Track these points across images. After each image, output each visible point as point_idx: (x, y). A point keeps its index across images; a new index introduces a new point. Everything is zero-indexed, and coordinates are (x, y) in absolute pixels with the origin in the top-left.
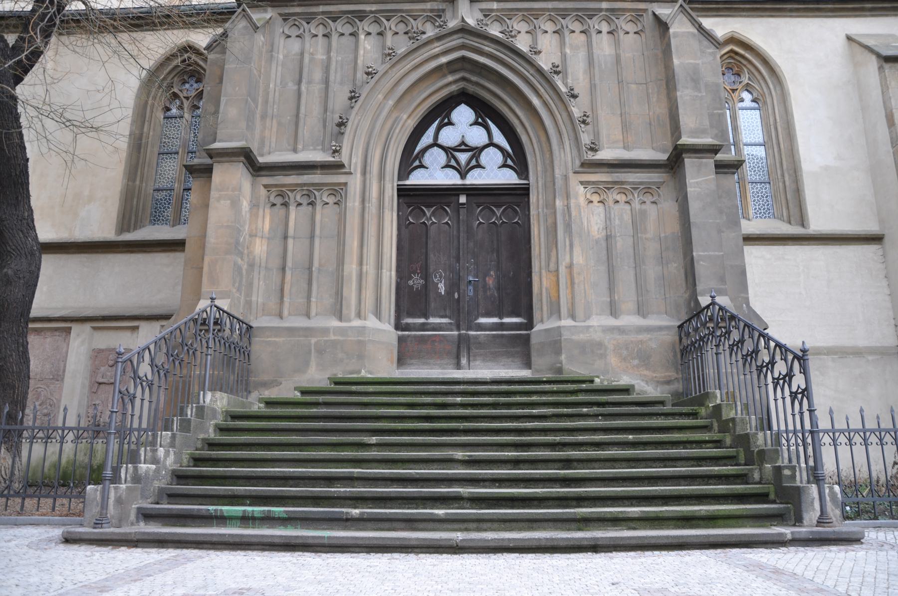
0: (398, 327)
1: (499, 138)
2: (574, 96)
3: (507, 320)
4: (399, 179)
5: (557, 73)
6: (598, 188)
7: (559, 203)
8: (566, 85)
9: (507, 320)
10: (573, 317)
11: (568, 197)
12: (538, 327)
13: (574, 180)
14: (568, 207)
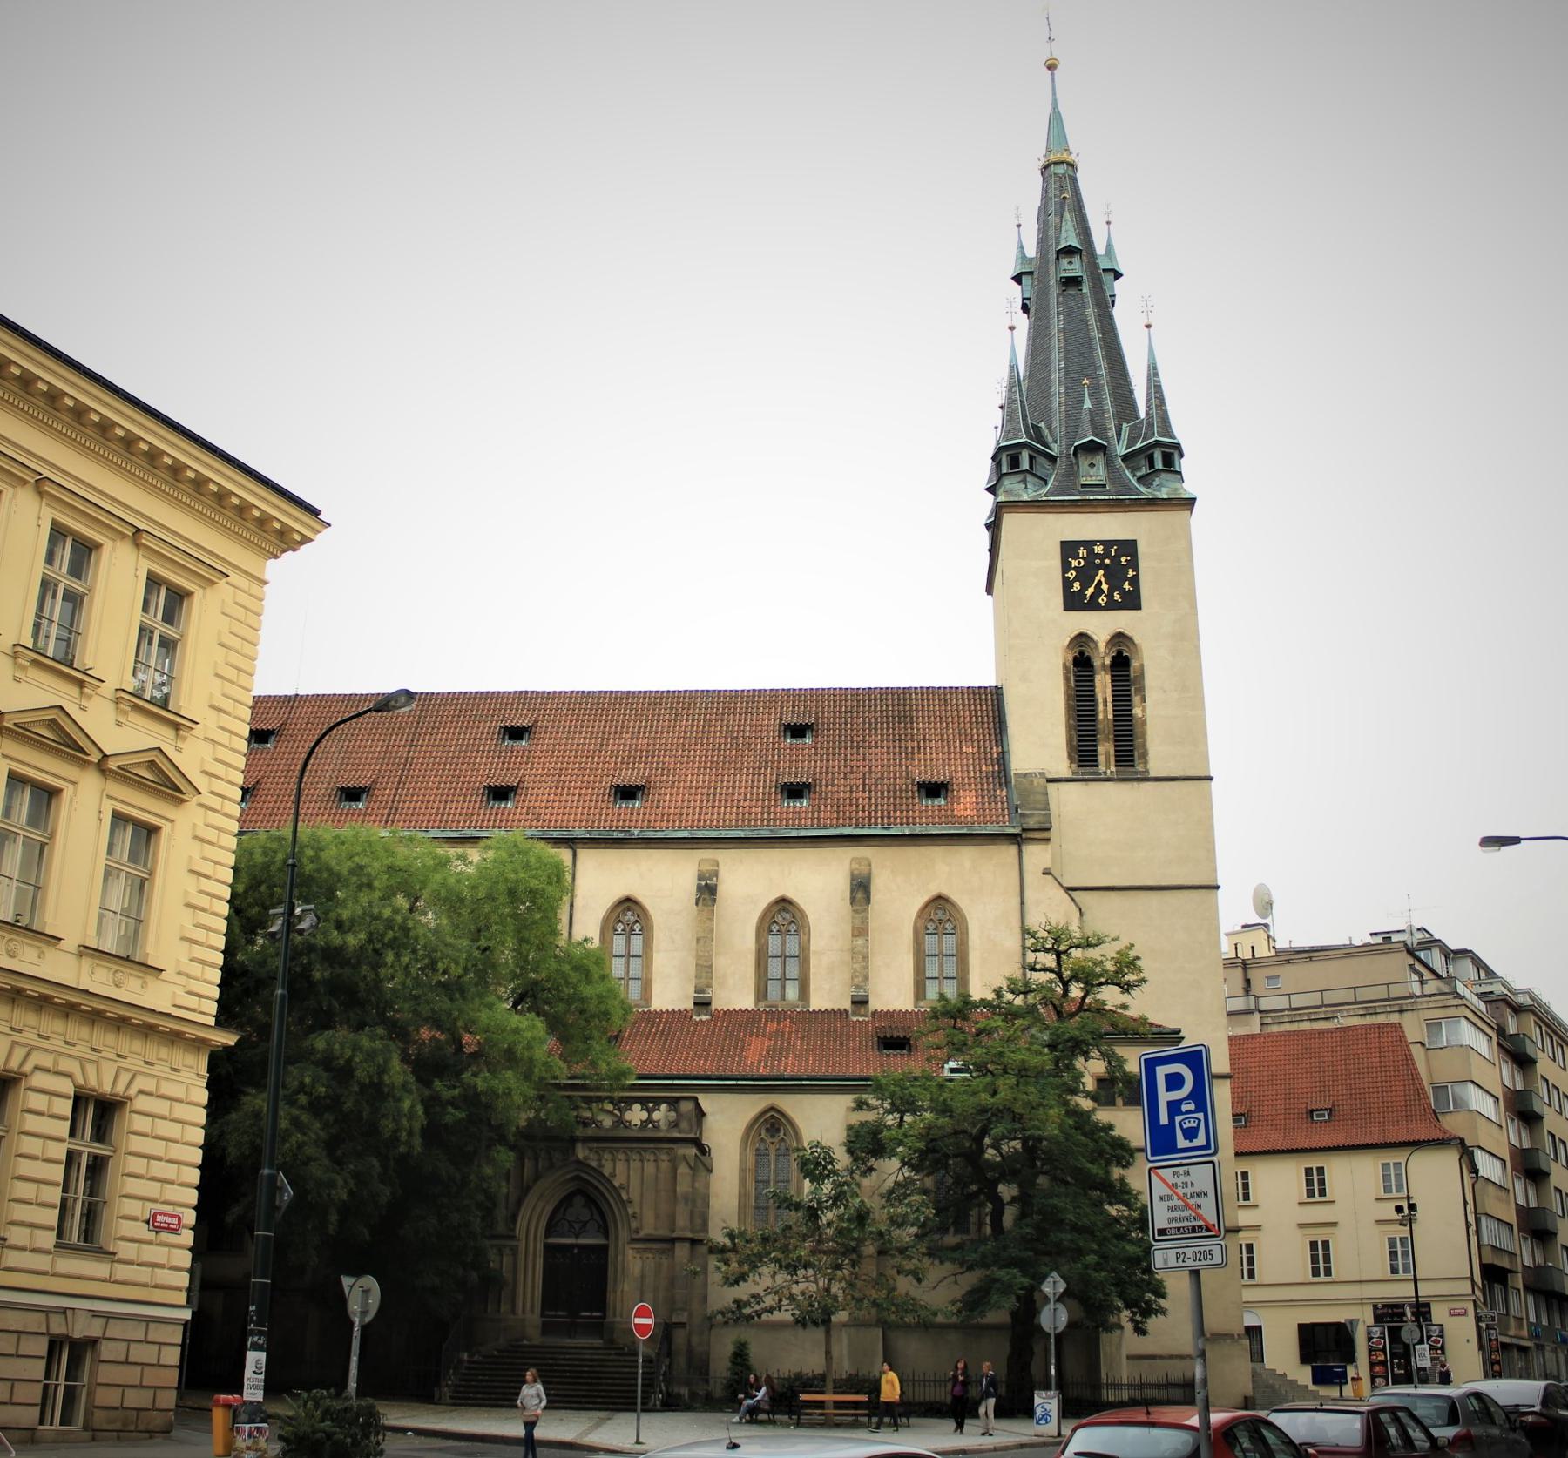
0: (542, 1315)
1: (597, 1217)
3: (595, 1314)
4: (547, 1235)
6: (638, 1251)
7: (620, 1258)
8: (628, 1193)
9: (595, 1314)
11: (624, 1255)
12: (607, 1320)
13: (627, 1247)
14: (623, 1261)
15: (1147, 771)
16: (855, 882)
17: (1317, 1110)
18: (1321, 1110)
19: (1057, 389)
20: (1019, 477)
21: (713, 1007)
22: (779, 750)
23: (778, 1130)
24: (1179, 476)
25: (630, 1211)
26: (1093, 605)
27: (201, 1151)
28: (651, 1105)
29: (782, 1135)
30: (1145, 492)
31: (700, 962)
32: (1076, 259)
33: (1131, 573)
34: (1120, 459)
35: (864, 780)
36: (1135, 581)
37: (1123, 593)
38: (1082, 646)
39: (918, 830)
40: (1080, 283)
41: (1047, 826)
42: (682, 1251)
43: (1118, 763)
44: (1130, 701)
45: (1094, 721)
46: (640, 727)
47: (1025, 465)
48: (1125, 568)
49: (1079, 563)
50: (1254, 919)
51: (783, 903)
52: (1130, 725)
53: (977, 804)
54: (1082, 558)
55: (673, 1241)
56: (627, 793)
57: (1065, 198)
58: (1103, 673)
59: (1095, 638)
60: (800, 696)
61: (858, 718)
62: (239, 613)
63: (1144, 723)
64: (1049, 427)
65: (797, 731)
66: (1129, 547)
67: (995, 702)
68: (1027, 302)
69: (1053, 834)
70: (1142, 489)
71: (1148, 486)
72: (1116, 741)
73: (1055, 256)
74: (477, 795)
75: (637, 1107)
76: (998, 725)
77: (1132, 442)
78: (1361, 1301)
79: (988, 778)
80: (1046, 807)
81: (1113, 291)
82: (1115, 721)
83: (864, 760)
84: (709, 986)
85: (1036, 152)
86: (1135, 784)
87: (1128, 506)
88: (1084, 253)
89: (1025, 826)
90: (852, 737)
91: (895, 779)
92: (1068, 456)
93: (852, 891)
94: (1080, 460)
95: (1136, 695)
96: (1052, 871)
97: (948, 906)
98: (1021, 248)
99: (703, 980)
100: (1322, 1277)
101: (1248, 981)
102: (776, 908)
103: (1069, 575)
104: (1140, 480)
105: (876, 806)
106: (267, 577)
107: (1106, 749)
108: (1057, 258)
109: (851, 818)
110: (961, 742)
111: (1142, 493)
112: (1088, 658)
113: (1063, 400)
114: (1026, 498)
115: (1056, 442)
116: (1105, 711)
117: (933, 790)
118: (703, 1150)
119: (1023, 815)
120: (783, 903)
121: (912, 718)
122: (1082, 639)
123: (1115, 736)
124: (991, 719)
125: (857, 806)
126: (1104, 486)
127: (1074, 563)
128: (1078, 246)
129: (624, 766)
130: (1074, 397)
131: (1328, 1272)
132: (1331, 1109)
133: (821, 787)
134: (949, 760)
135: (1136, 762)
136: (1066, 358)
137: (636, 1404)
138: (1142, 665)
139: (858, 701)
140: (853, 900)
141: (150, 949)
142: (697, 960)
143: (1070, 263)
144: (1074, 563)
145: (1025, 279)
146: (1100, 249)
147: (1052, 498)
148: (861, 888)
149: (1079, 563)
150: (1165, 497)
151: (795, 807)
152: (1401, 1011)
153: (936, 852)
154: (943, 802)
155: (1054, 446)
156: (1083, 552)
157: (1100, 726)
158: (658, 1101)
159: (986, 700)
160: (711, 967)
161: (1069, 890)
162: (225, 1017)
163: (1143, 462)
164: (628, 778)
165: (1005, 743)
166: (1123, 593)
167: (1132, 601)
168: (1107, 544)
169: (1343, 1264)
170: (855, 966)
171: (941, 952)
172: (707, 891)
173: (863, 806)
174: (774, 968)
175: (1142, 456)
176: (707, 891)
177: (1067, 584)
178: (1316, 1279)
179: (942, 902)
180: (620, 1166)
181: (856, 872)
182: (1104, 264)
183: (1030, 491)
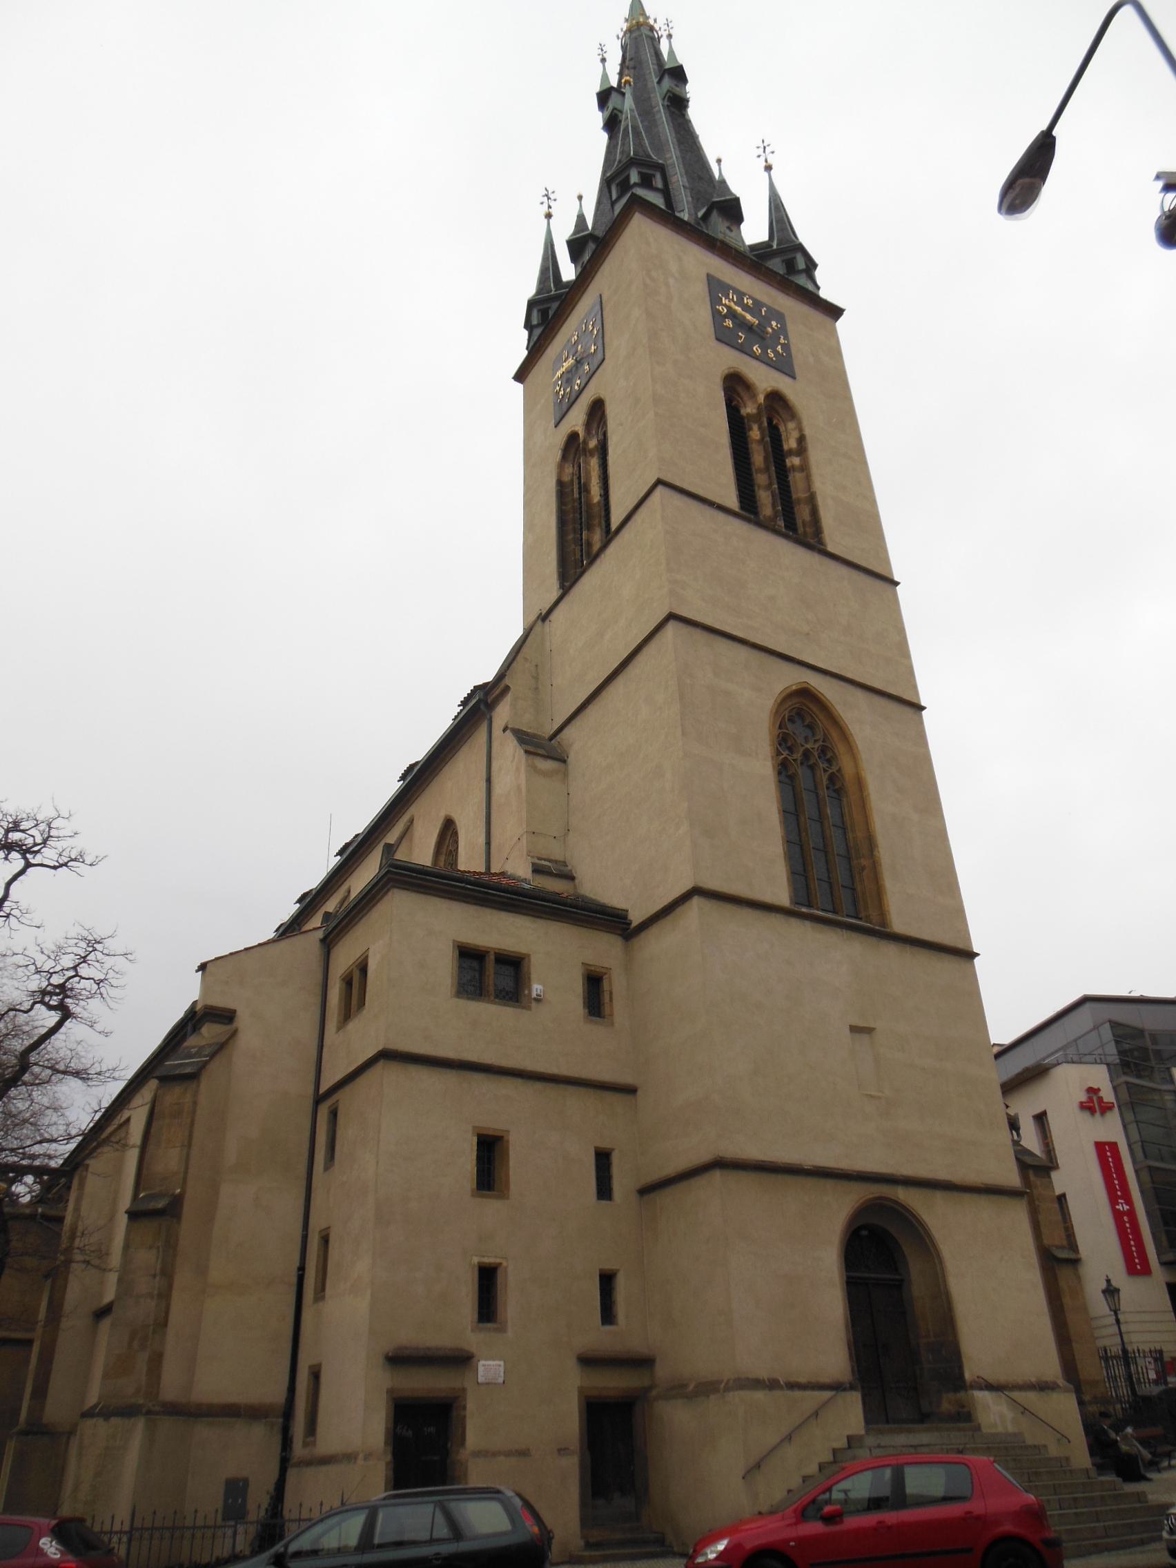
33: (782, 341)
168: (755, 301)
177: (717, 316)
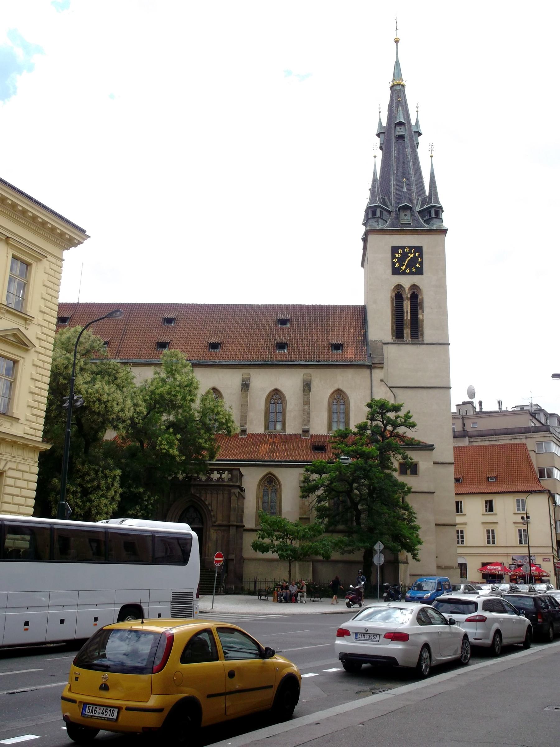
2: (212, 510)
5: (210, 505)
7: (208, 533)
10: (208, 557)
15: (423, 341)
16: (305, 383)
17: (490, 477)
18: (492, 477)
19: (393, 183)
20: (376, 220)
21: (248, 432)
22: (276, 329)
23: (272, 482)
24: (441, 220)
25: (212, 514)
26: (404, 273)
27: (35, 492)
28: (221, 472)
29: (273, 484)
30: (427, 227)
31: (242, 414)
32: (403, 127)
33: (420, 260)
34: (417, 213)
35: (310, 342)
36: (421, 263)
37: (416, 268)
38: (398, 289)
39: (330, 363)
40: (404, 138)
41: (383, 362)
42: (233, 531)
43: (412, 337)
44: (417, 312)
45: (402, 320)
46: (220, 319)
47: (378, 215)
48: (418, 258)
49: (399, 255)
50: (468, 400)
51: (276, 391)
52: (417, 322)
53: (355, 352)
54: (400, 253)
55: (229, 526)
56: (214, 346)
57: (399, 100)
58: (407, 300)
59: (404, 286)
60: (285, 308)
61: (308, 317)
62: (52, 273)
63: (423, 321)
64: (389, 199)
65: (283, 322)
66: (419, 250)
67: (363, 311)
68: (382, 145)
69: (385, 365)
70: (426, 225)
71: (428, 224)
72: (411, 328)
73: (394, 126)
74: (153, 346)
75: (215, 472)
76: (364, 321)
77: (422, 205)
78: (507, 555)
79: (359, 342)
80: (382, 354)
81: (418, 141)
82: (411, 320)
83: (310, 334)
84: (246, 424)
85: (388, 80)
86: (418, 346)
87: (419, 232)
88: (406, 125)
89: (373, 362)
90: (305, 325)
91: (322, 342)
92: (396, 211)
93: (304, 386)
94: (401, 212)
95: (420, 310)
96: (384, 380)
97: (342, 393)
98: (380, 122)
99: (243, 421)
100: (491, 544)
101: (464, 425)
102: (273, 393)
103: (394, 260)
104: (425, 221)
105: (314, 353)
106: (64, 258)
107: (407, 331)
108: (395, 127)
109: (304, 357)
110: (349, 328)
111: (426, 227)
112: (401, 295)
113: (395, 187)
114: (378, 228)
115: (391, 205)
116: (407, 316)
117: (337, 347)
118: (242, 490)
119: (373, 358)
120: (276, 391)
121: (329, 317)
122: (399, 288)
123: (411, 326)
124: (361, 318)
125: (307, 352)
126: (410, 224)
127: (397, 256)
128: (404, 122)
129: (213, 335)
130: (399, 186)
131: (494, 542)
132: (496, 477)
133: (292, 345)
134: (344, 335)
135: (419, 337)
136: (397, 170)
137: (213, 592)
138: (423, 298)
139: (308, 310)
140: (304, 391)
141: (14, 411)
142: (241, 413)
143: (401, 129)
144: (397, 256)
145: (382, 135)
146: (413, 123)
147: (389, 229)
148: (307, 386)
149: (399, 255)
150: (435, 229)
151: (281, 353)
152: (526, 438)
153: (338, 371)
154: (341, 351)
155: (390, 207)
156: (400, 251)
157: (405, 322)
158: (224, 470)
159: (360, 311)
160: (247, 416)
161: (390, 388)
162: (45, 439)
163: (426, 214)
164: (214, 340)
165: (366, 328)
166: (416, 268)
167: (420, 272)
168: (410, 248)
169: (500, 539)
170: (304, 417)
171: (339, 411)
172: (245, 386)
173: (309, 353)
174: (272, 417)
175: (426, 211)
176: (245, 386)
177: (393, 264)
178: (489, 545)
179: (339, 392)
180: (209, 496)
181: (305, 379)
182: (414, 130)
183: (379, 226)
